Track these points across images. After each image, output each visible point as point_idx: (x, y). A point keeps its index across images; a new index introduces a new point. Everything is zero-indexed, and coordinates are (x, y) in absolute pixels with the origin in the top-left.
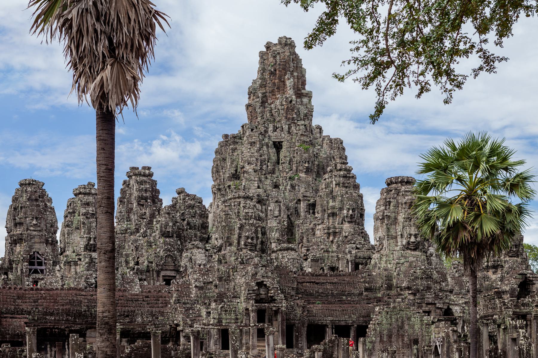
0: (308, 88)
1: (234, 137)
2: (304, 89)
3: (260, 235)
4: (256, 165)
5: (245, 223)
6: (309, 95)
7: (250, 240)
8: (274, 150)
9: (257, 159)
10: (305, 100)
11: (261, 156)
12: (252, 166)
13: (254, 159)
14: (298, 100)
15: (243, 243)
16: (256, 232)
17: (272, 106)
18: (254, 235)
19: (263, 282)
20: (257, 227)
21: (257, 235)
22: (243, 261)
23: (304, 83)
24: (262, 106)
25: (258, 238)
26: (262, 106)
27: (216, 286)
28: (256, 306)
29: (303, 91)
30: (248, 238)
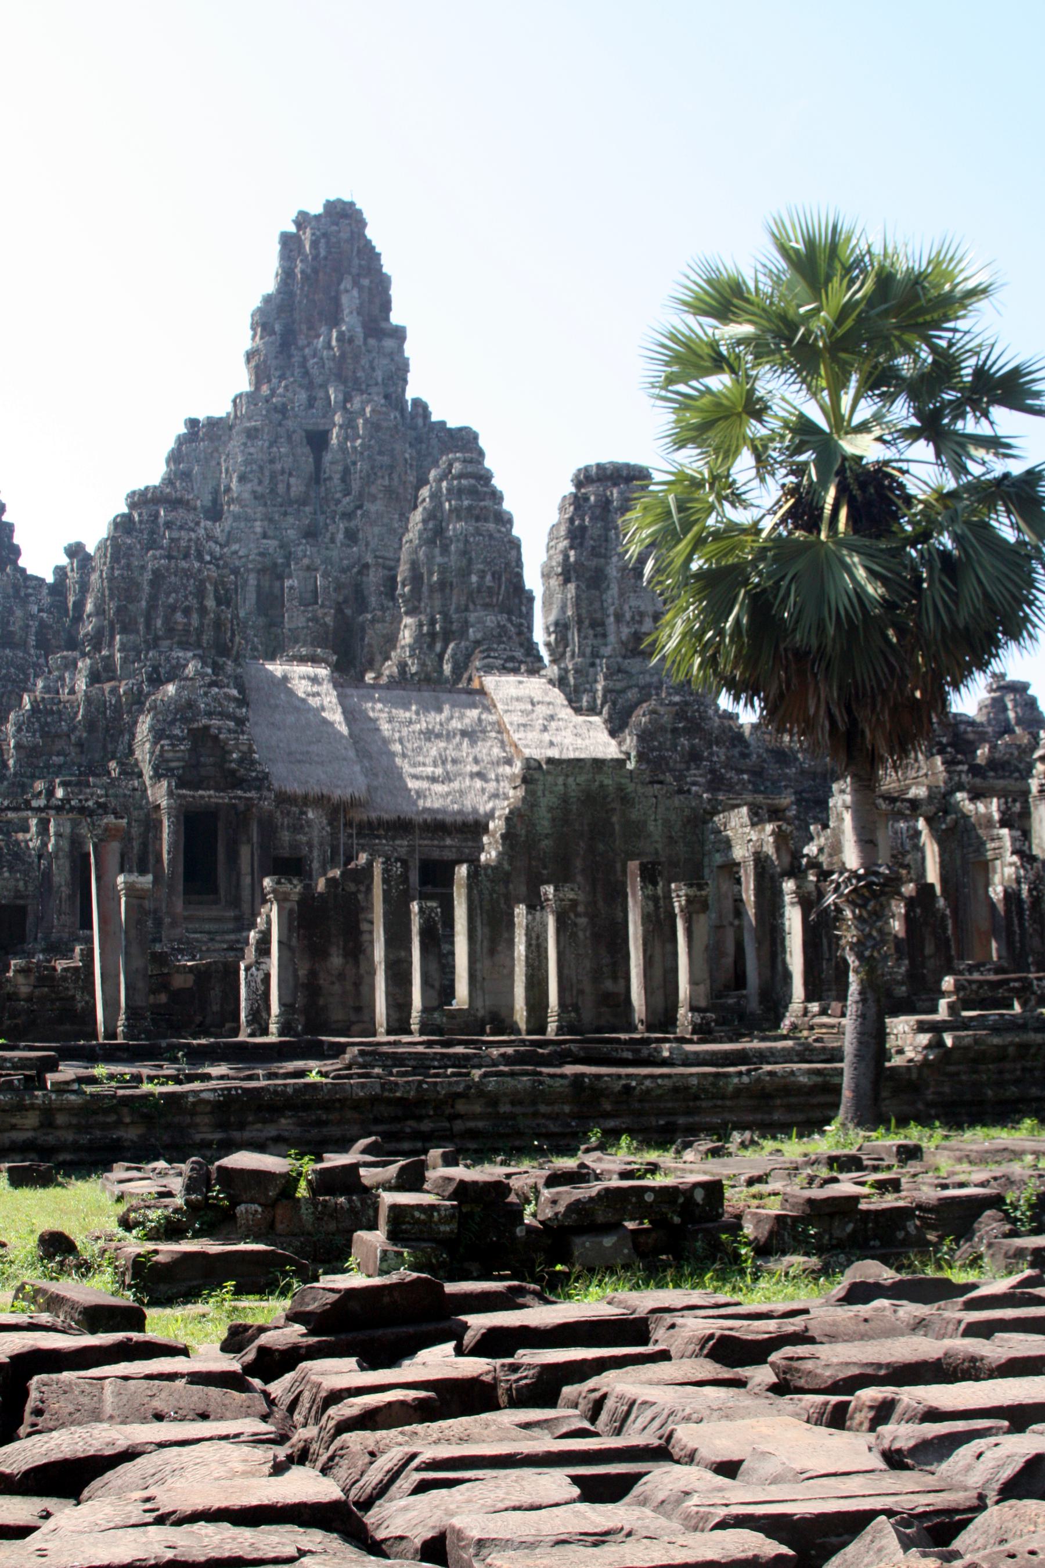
0: (396, 318)
1: (213, 423)
2: (387, 319)
3: (210, 603)
4: (260, 483)
5: (168, 569)
6: (399, 334)
7: (179, 617)
8: (307, 450)
9: (261, 468)
10: (389, 343)
11: (272, 461)
12: (249, 485)
13: (254, 467)
14: (372, 342)
15: (159, 623)
16: (201, 594)
17: (307, 351)
18: (192, 601)
19: (207, 728)
20: (202, 582)
21: (201, 603)
22: (159, 674)
23: (386, 306)
24: (281, 352)
25: (203, 611)
26: (281, 352)
27: (80, 744)
28: (179, 796)
29: (383, 325)
30: (173, 608)
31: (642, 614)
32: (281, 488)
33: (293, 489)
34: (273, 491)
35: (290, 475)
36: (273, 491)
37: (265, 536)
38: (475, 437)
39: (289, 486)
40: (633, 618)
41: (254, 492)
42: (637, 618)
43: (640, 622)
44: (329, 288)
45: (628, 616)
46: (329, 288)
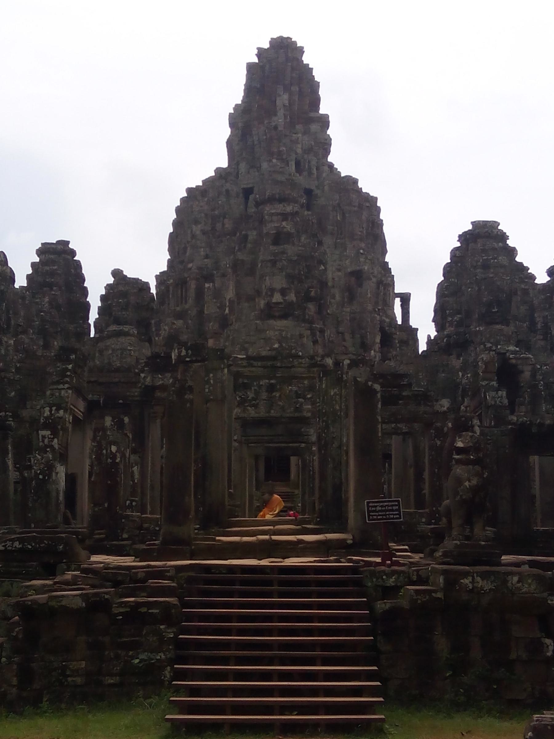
0: (322, 111)
9: (206, 215)
10: (314, 127)
11: (213, 210)
12: (199, 226)
13: (203, 215)
31: (272, 291)
32: (219, 226)
33: (227, 226)
34: (213, 229)
35: (224, 218)
36: (213, 229)
37: (207, 257)
38: (355, 181)
39: (223, 225)
40: (266, 293)
41: (202, 230)
42: (269, 293)
43: (272, 296)
44: (280, 95)
45: (264, 291)
46: (280, 95)
